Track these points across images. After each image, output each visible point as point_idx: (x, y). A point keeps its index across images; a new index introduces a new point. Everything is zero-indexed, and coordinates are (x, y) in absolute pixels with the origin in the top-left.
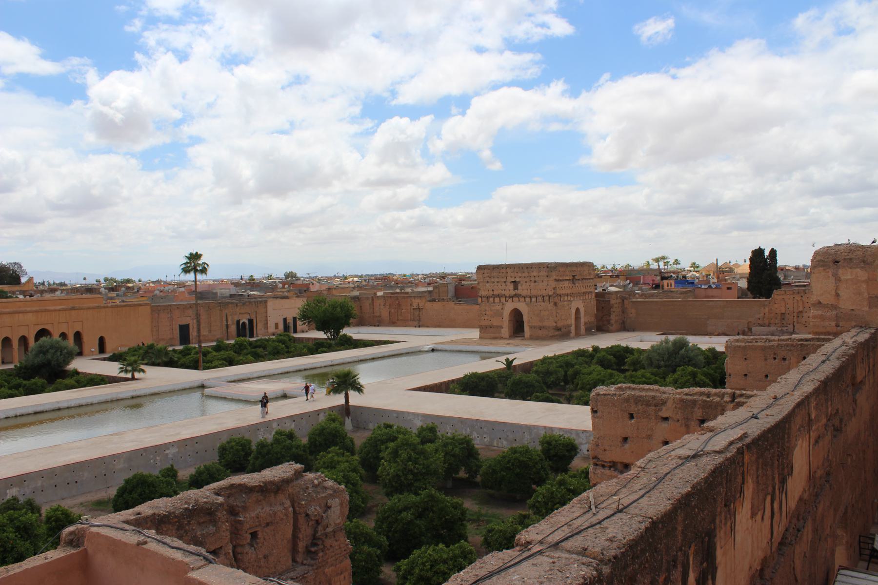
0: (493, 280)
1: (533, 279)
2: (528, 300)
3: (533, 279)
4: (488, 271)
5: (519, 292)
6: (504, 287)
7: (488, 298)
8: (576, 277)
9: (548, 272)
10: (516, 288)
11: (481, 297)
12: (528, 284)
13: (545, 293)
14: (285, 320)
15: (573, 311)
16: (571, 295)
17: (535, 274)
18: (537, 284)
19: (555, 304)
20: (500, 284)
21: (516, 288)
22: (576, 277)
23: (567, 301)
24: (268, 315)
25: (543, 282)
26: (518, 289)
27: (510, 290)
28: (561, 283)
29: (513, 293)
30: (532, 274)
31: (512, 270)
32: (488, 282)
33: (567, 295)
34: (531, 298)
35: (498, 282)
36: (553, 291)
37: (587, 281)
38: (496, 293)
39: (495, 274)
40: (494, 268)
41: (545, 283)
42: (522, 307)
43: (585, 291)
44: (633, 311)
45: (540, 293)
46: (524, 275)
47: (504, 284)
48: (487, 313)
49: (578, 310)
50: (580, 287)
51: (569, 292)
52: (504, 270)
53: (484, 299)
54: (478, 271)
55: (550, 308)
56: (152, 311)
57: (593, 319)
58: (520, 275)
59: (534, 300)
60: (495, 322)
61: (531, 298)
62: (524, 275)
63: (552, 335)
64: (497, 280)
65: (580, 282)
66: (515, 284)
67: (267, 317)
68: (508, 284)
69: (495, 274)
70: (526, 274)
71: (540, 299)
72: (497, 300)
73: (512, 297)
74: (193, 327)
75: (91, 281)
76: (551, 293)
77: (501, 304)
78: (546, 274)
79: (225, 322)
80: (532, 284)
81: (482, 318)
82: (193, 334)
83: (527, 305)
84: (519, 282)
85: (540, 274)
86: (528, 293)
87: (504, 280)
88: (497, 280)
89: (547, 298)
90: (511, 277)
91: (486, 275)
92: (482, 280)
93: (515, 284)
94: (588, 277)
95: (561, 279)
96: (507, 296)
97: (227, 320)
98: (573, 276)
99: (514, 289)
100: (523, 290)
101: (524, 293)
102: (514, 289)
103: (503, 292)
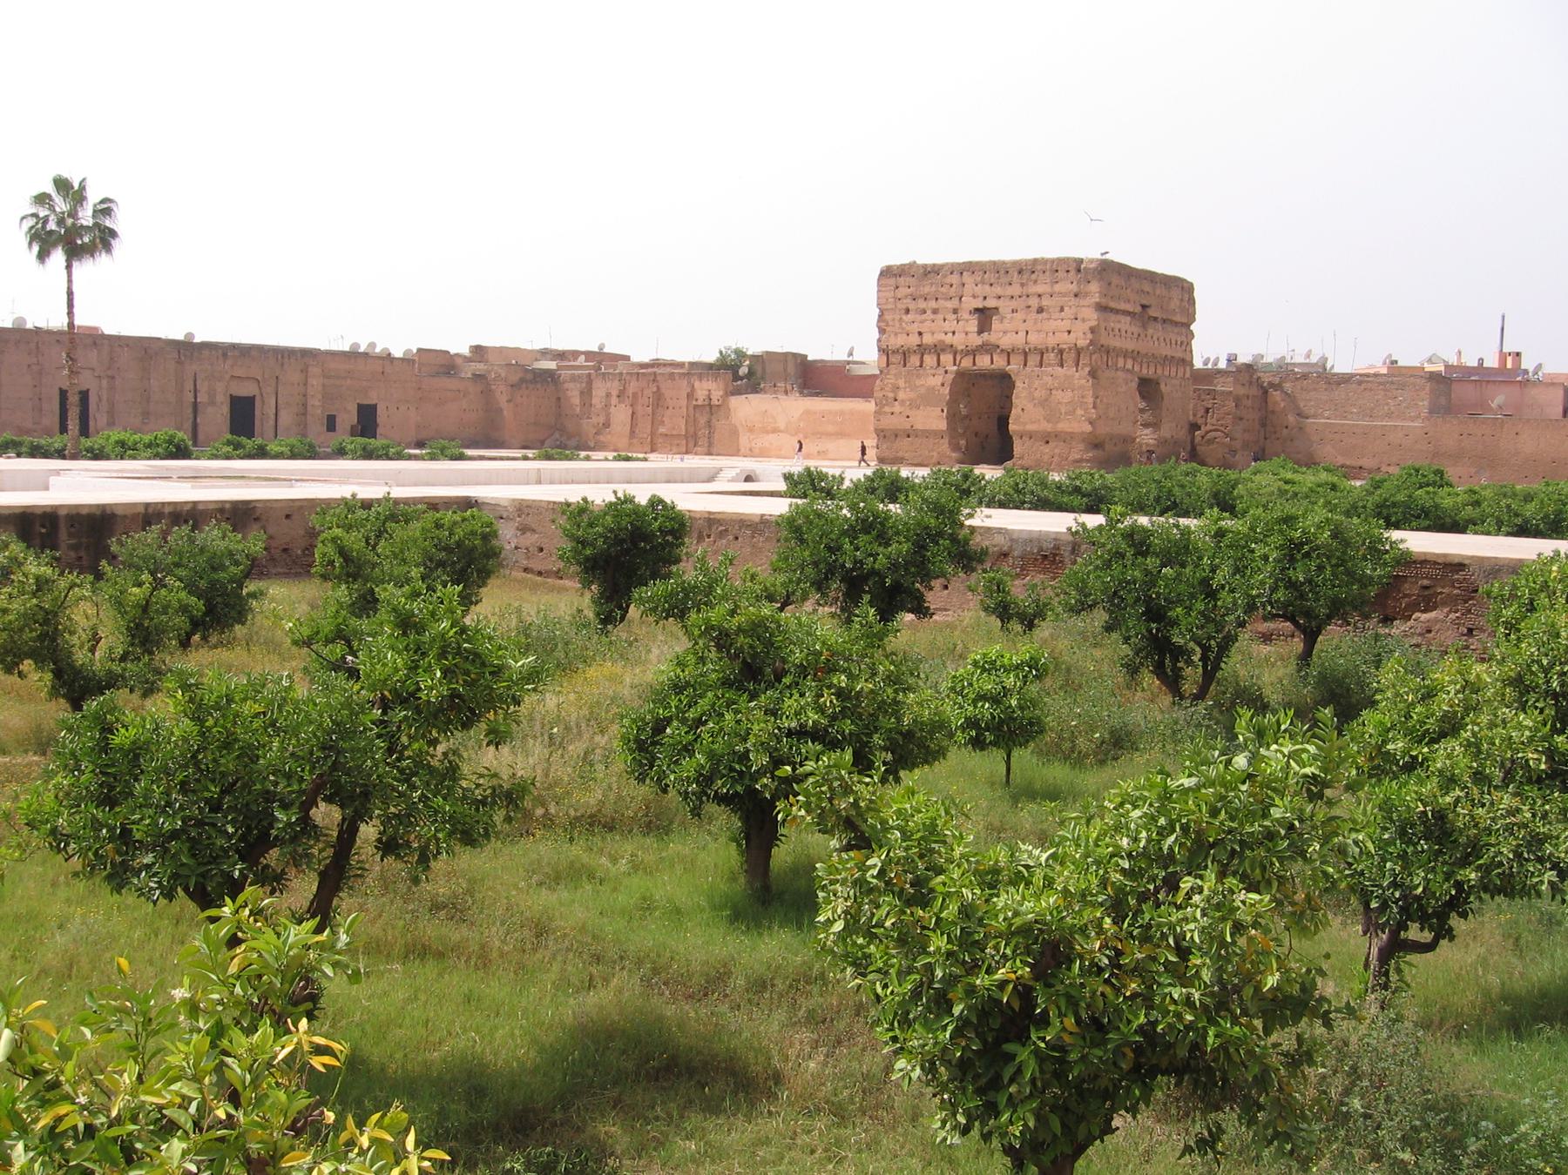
0: (922, 304)
1: (1034, 302)
3: (1034, 302)
4: (909, 280)
5: (995, 336)
7: (905, 354)
9: (1079, 282)
10: (984, 327)
12: (1019, 316)
13: (1064, 340)
17: (1040, 289)
18: (1044, 315)
19: (1093, 374)
20: (940, 316)
21: (984, 327)
23: (1124, 369)
25: (1062, 309)
28: (1113, 317)
29: (976, 340)
32: (907, 311)
35: (935, 311)
36: (1090, 336)
38: (928, 339)
45: (1051, 341)
46: (1010, 291)
48: (901, 395)
52: (955, 279)
53: (893, 359)
58: (998, 290)
59: (1033, 359)
62: (1010, 291)
63: (1078, 457)
64: (933, 304)
66: (985, 316)
69: (927, 289)
70: (1016, 290)
71: (1051, 357)
72: (930, 360)
76: (1082, 343)
77: (941, 371)
78: (1074, 288)
81: (887, 409)
85: (1057, 288)
86: (1019, 340)
87: (954, 303)
88: (933, 304)
89: (1073, 354)
90: (974, 297)
91: (903, 291)
93: (985, 316)
95: (1112, 305)
96: (960, 348)
99: (980, 332)
101: (1006, 341)
102: (980, 332)
103: (949, 339)
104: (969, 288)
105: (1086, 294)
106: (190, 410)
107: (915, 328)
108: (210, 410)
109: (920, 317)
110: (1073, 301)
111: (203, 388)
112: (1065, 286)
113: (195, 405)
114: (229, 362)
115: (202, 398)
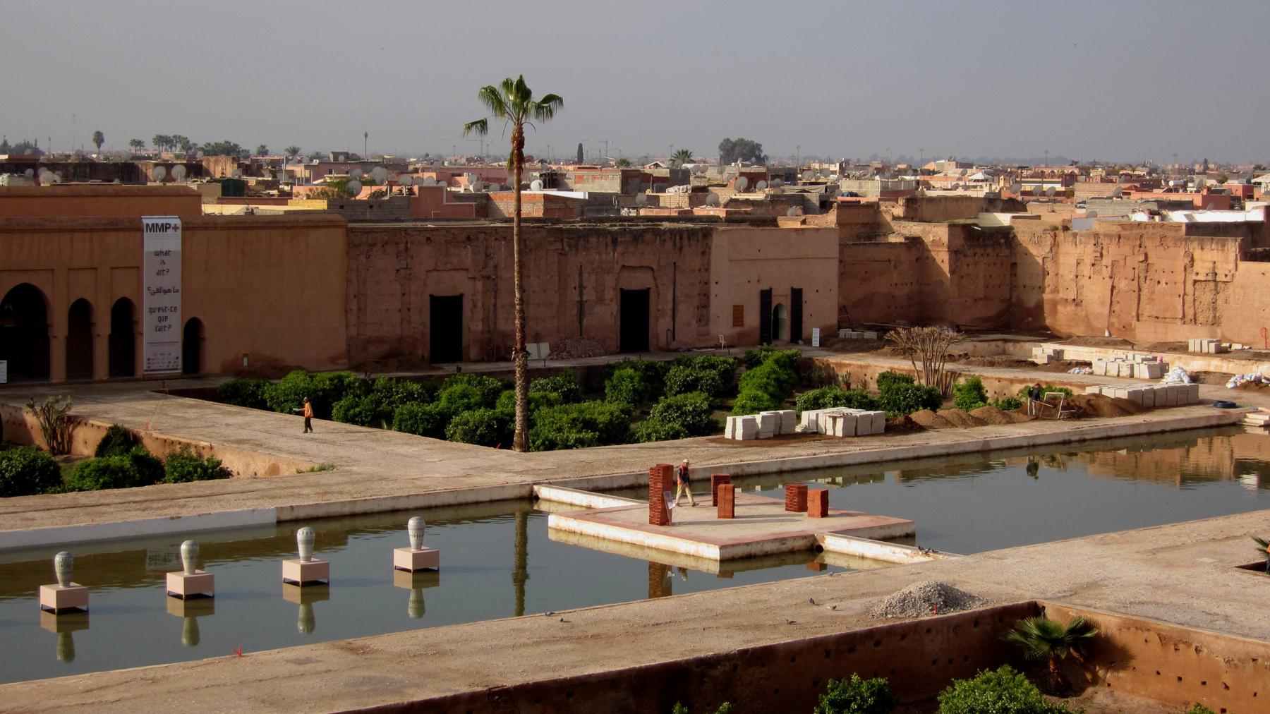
14: (766, 296)
24: (713, 278)
56: (351, 246)
74: (475, 306)
75: (117, 146)
79: (576, 293)
82: (473, 327)
97: (581, 287)
106: (575, 311)
108: (598, 309)
111: (590, 281)
113: (581, 304)
114: (620, 249)
115: (589, 295)
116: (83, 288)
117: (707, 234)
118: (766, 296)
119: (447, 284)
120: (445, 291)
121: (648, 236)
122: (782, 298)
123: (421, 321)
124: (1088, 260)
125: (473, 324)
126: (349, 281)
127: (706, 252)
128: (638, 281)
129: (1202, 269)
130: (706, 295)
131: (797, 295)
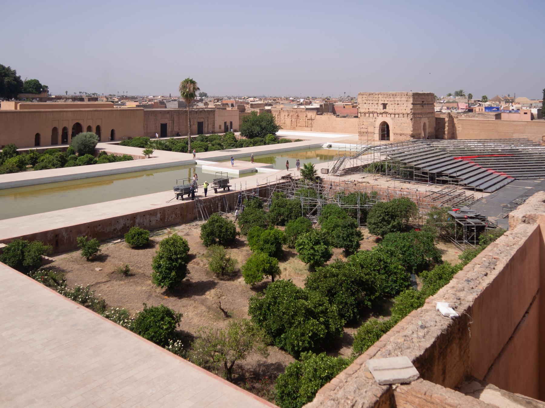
0: (369, 102)
2: (393, 116)
3: (396, 102)
6: (376, 107)
8: (425, 103)
11: (360, 113)
12: (393, 106)
13: (404, 112)
14: (225, 123)
15: (422, 124)
16: (421, 114)
17: (398, 99)
20: (373, 105)
22: (425, 103)
26: (386, 108)
27: (380, 109)
28: (416, 106)
29: (382, 111)
30: (396, 99)
31: (382, 96)
32: (365, 103)
33: (419, 114)
34: (395, 114)
35: (372, 104)
37: (431, 105)
38: (371, 110)
39: (370, 98)
40: (370, 95)
41: (405, 105)
42: (389, 120)
43: (429, 111)
44: (460, 126)
45: (401, 112)
47: (376, 105)
49: (425, 124)
50: (426, 109)
51: (420, 112)
52: (377, 96)
54: (359, 96)
55: (408, 122)
57: (433, 130)
58: (388, 99)
59: (397, 116)
60: (370, 130)
61: (395, 114)
62: (390, 99)
64: (372, 102)
65: (426, 105)
66: (385, 106)
67: (214, 121)
68: (379, 105)
69: (370, 98)
70: (392, 99)
71: (401, 115)
72: (371, 115)
73: (382, 114)
76: (409, 112)
77: (374, 118)
78: (406, 99)
80: (396, 106)
83: (392, 119)
84: (387, 104)
85: (402, 99)
86: (393, 111)
87: (377, 102)
88: (372, 102)
89: (406, 115)
92: (361, 102)
93: (385, 106)
94: (431, 103)
95: (415, 103)
98: (423, 102)
99: (383, 109)
100: (389, 109)
101: (390, 111)
102: (383, 109)
103: (376, 110)
104: (380, 99)
105: (409, 101)
107: (368, 107)
108: (193, 126)
109: (368, 105)
110: (406, 102)
111: (192, 121)
112: (404, 99)
114: (197, 114)
115: (192, 123)
116: (90, 123)
117: (214, 111)
118: (225, 123)
119: (164, 121)
120: (163, 123)
121: (203, 112)
122: (228, 124)
123: (159, 129)
124: (287, 115)
125: (169, 129)
126: (144, 121)
127: (214, 115)
128: (201, 120)
129: (309, 117)
130: (214, 123)
131: (231, 123)
